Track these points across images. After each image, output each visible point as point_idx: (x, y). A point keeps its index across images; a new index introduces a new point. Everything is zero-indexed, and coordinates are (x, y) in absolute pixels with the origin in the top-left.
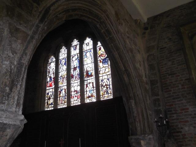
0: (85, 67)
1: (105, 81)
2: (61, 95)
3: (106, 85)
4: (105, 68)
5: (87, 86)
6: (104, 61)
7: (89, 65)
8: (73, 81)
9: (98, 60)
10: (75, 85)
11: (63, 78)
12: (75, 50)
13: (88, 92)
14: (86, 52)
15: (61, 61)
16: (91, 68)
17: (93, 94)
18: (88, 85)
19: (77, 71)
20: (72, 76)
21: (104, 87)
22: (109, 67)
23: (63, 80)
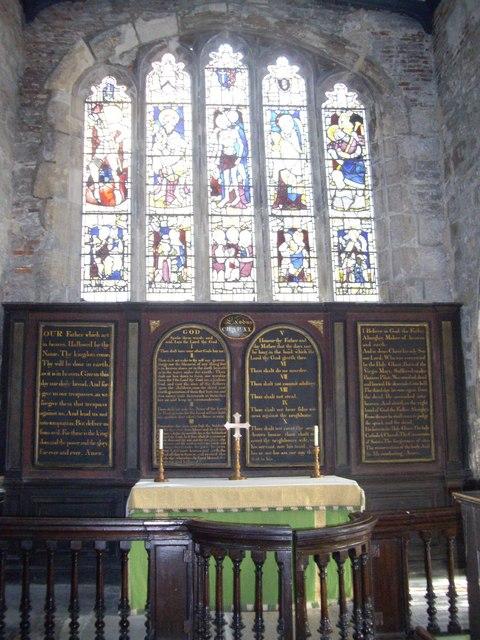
0: (273, 168)
1: (353, 235)
2: (164, 248)
3: (355, 250)
4: (354, 192)
5: (281, 239)
6: (351, 167)
7: (288, 164)
8: (221, 204)
9: (327, 156)
10: (227, 222)
11: (173, 185)
12: (228, 86)
13: (286, 262)
14: (278, 112)
15: (157, 112)
16: (299, 179)
17: (308, 271)
18: (287, 236)
19: (238, 174)
20: (217, 189)
21: (349, 255)
22: (369, 194)
23: (170, 193)
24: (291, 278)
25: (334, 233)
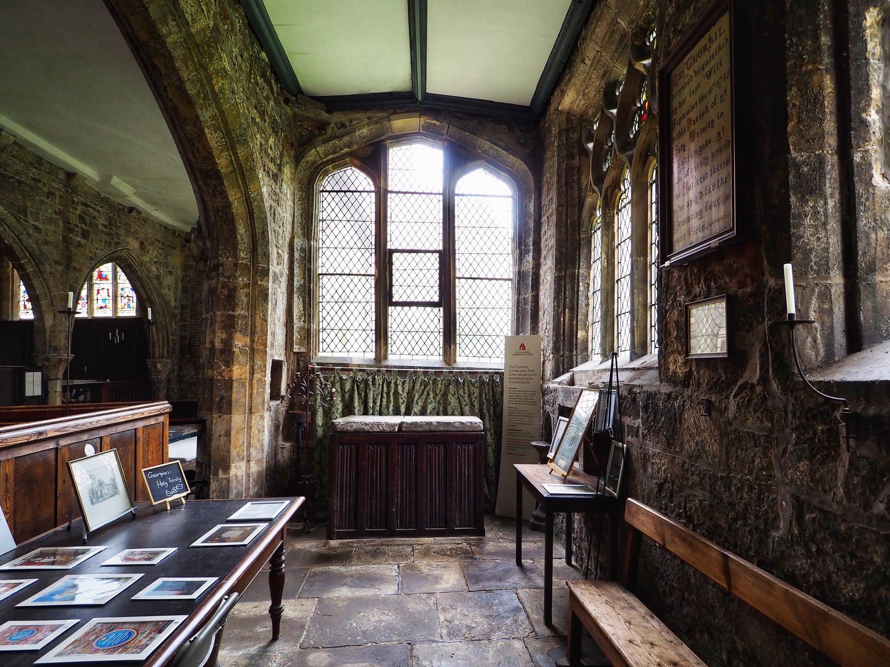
5: (98, 293)
24: (101, 308)
25: (119, 289)
